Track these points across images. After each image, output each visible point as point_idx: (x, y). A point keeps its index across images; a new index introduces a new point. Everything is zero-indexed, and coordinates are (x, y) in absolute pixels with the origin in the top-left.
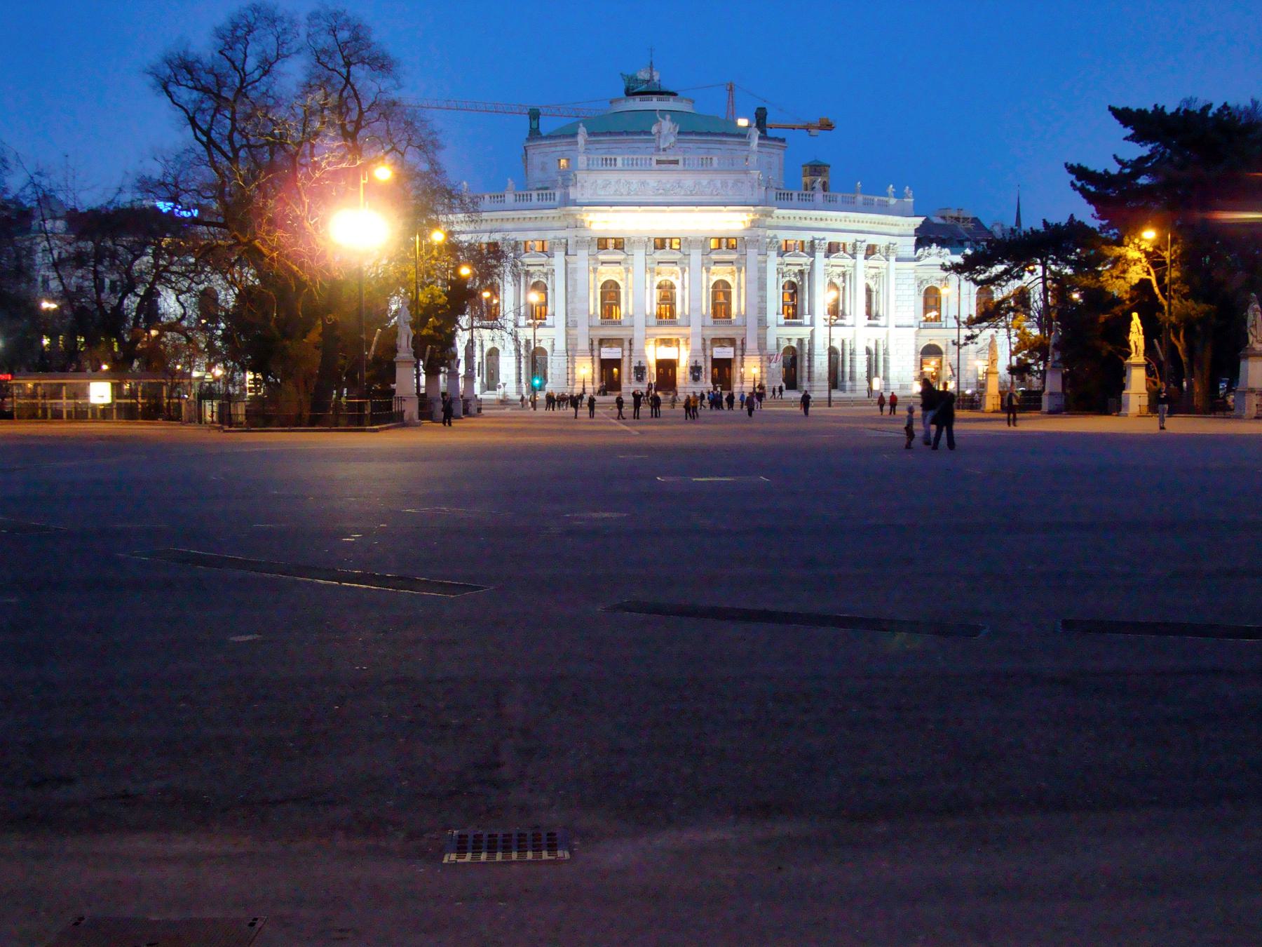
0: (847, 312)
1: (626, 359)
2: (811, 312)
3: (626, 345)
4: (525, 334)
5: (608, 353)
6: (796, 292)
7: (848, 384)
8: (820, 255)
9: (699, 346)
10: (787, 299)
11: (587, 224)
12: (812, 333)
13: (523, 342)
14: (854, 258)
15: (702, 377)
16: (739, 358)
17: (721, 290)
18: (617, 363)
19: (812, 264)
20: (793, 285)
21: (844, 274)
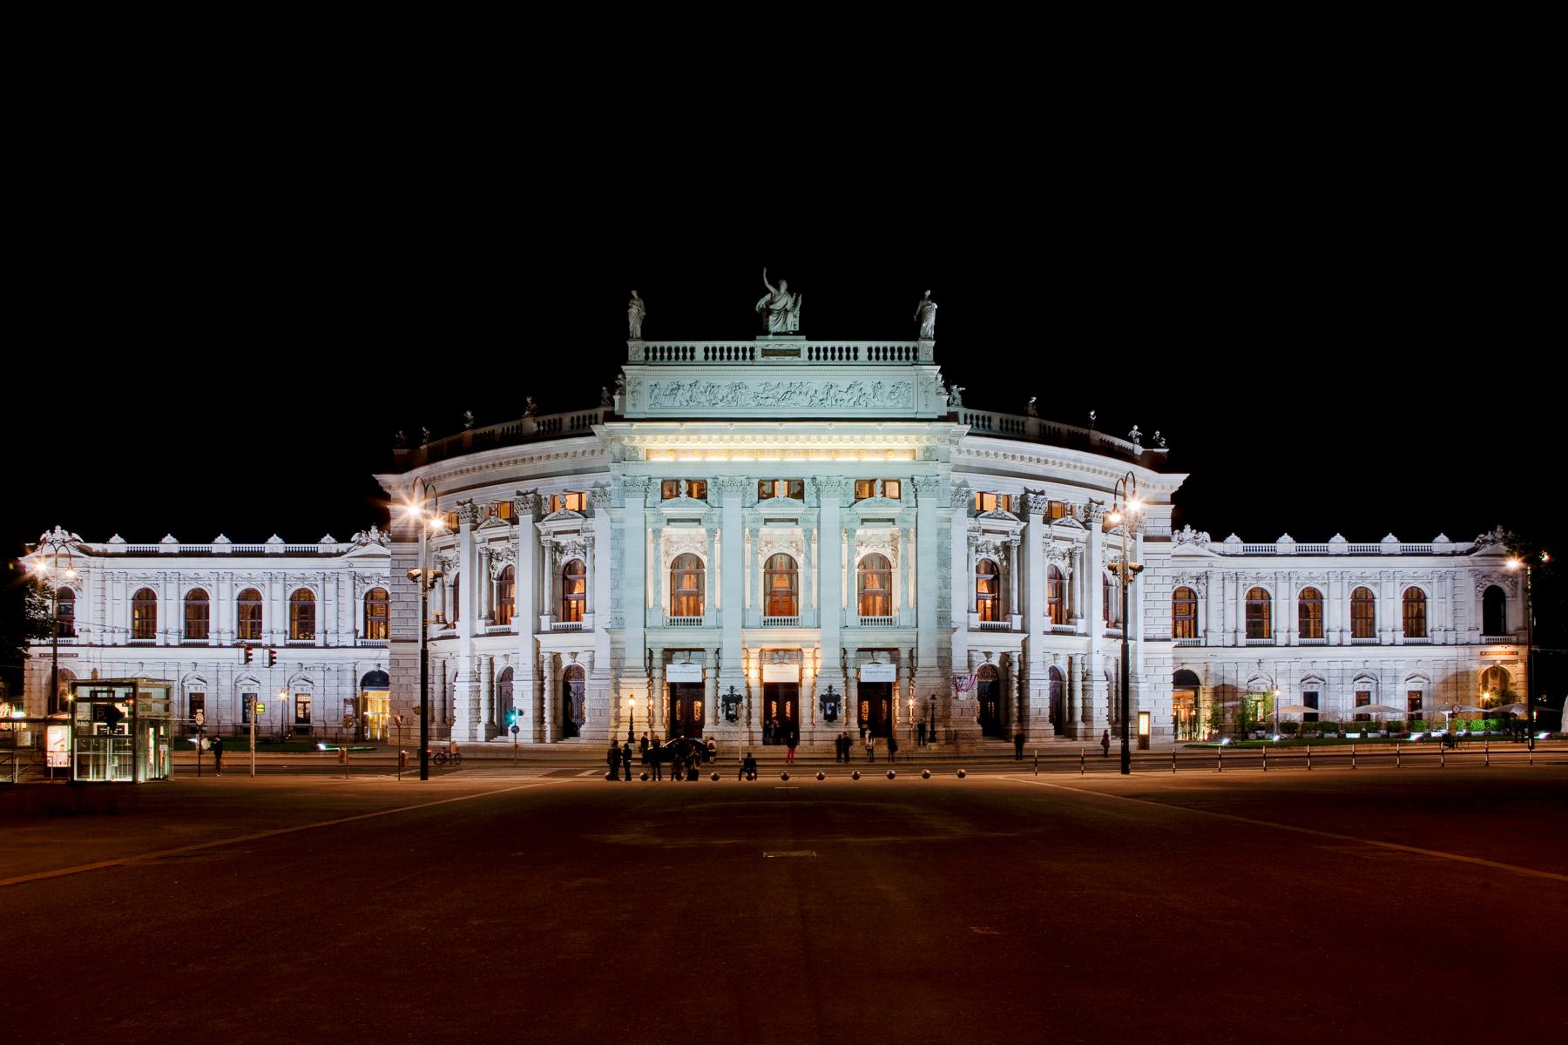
0: (1077, 612)
1: (709, 685)
2: (1023, 611)
3: (710, 656)
4: (550, 643)
5: (680, 673)
6: (997, 578)
7: (1080, 726)
8: (1036, 519)
10: (984, 589)
11: (642, 456)
12: (1025, 644)
13: (547, 658)
14: (1088, 528)
15: (841, 714)
17: (878, 572)
18: (696, 689)
19: (1023, 534)
20: (992, 567)
21: (1071, 554)
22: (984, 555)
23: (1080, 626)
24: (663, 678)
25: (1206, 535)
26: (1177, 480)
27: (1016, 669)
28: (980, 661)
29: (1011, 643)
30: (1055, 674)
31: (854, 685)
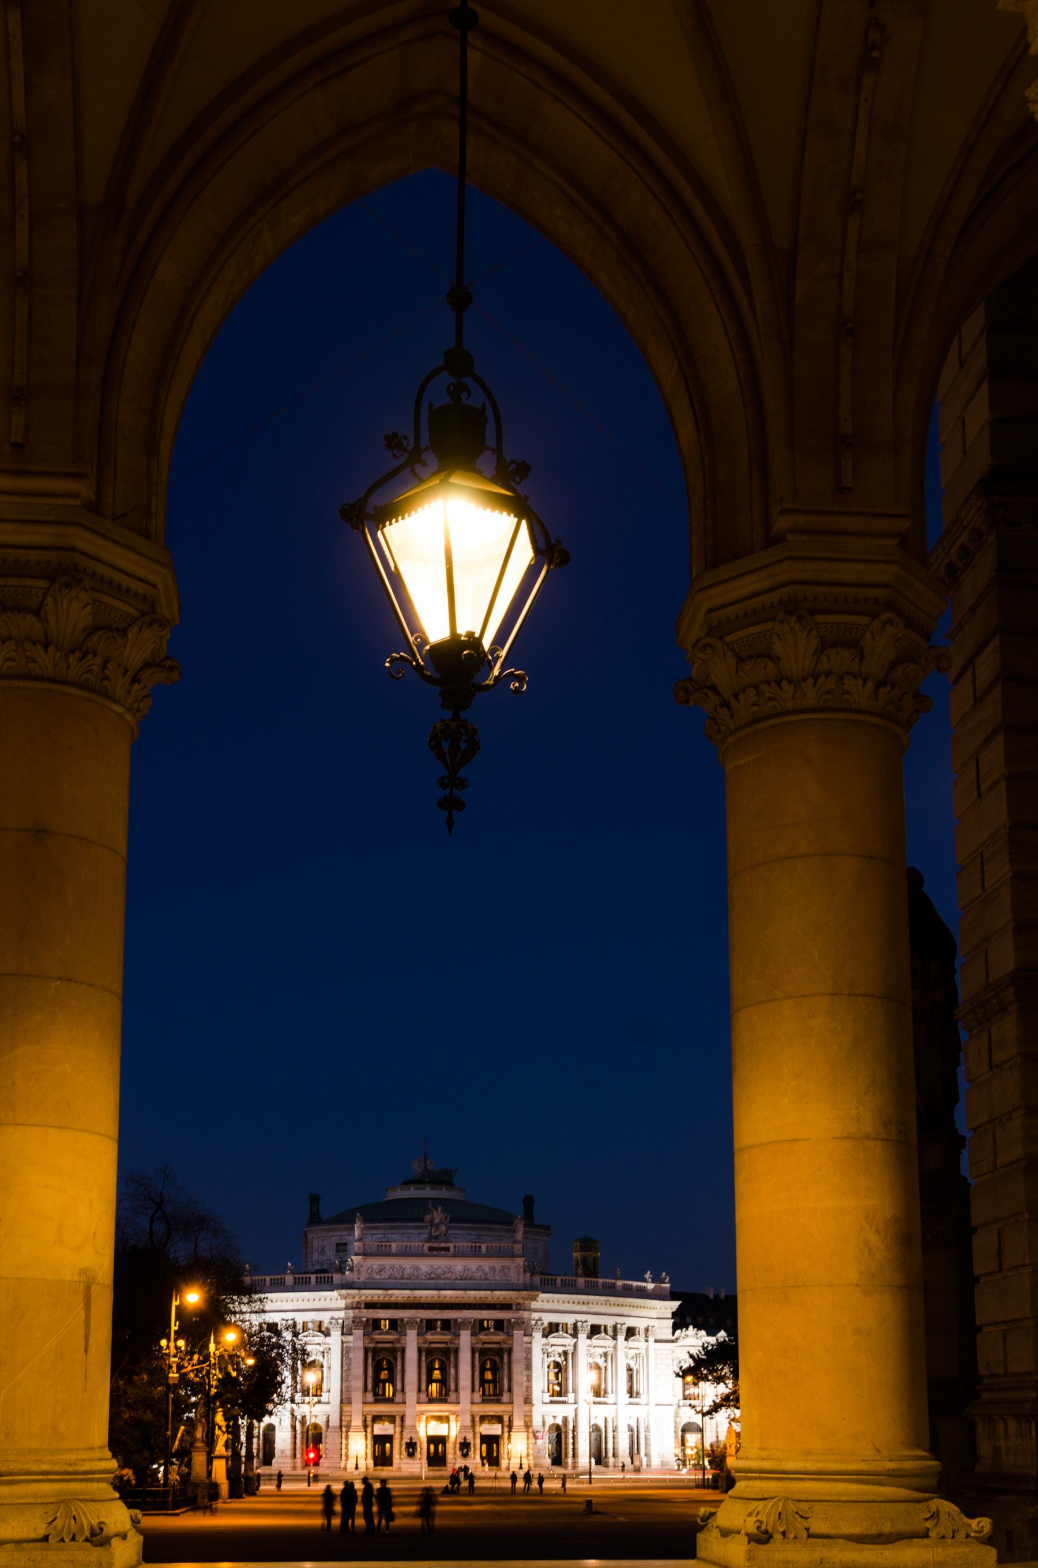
0: (609, 1390)
3: (398, 1420)
5: (379, 1429)
6: (560, 1371)
8: (582, 1336)
9: (468, 1423)
10: (552, 1377)
12: (576, 1410)
15: (471, 1454)
16: (506, 1435)
18: (389, 1438)
19: (575, 1345)
20: (557, 1365)
21: (606, 1355)
22: (552, 1359)
23: (611, 1398)
24: (372, 1431)
25: (703, 1333)
26: (675, 1304)
27: (571, 1427)
28: (550, 1421)
29: (567, 1411)
30: (596, 1429)
31: (478, 1436)
